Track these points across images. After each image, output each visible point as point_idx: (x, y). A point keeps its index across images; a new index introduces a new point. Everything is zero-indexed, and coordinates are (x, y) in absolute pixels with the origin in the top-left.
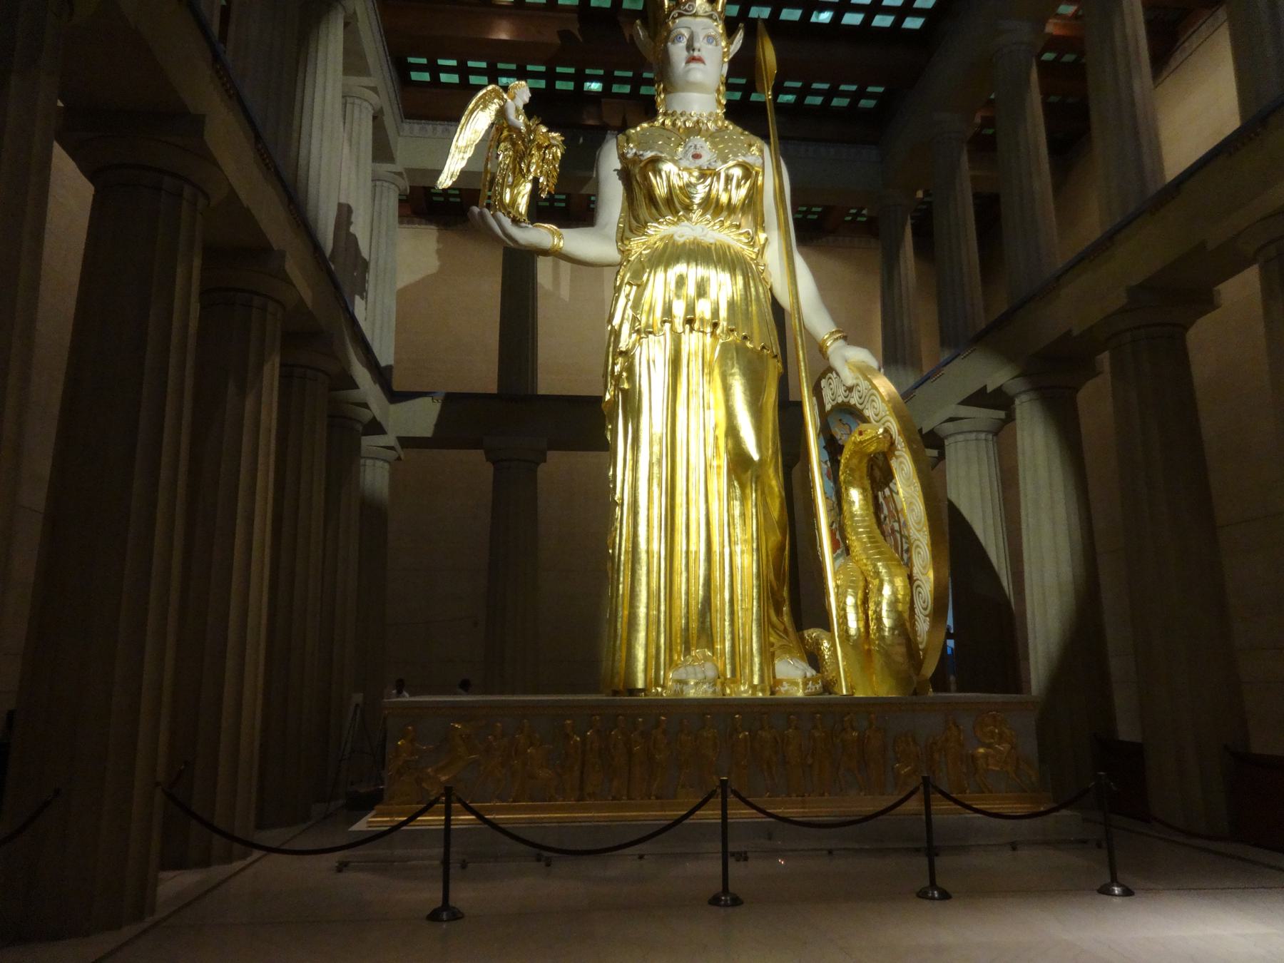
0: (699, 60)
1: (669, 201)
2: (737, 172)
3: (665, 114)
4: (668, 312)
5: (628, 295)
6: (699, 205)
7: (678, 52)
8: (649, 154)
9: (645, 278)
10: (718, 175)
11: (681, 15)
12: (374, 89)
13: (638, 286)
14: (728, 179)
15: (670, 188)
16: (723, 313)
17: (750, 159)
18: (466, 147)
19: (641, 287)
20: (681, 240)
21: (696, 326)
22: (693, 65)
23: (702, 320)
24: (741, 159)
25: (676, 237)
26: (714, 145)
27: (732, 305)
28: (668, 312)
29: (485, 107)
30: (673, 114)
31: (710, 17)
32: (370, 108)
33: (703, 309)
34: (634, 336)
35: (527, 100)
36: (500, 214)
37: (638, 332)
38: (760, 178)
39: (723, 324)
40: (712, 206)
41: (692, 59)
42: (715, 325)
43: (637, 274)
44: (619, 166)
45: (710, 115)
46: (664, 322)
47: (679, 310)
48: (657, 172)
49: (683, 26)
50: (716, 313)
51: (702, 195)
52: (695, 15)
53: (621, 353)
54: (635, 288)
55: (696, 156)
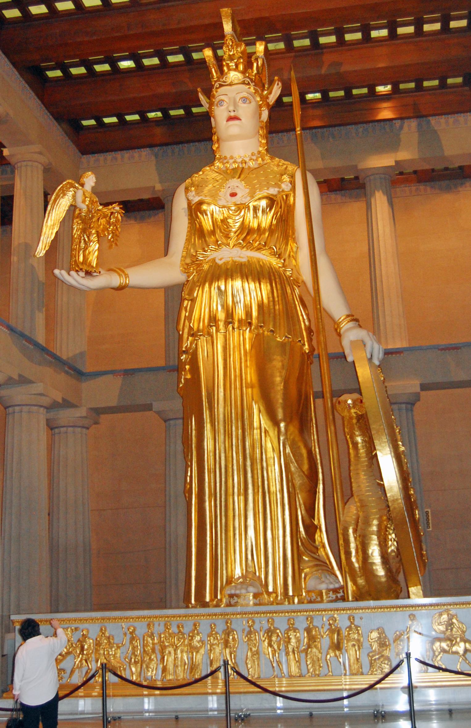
0: (236, 118)
1: (213, 233)
2: (263, 203)
3: (220, 159)
4: (213, 319)
5: (186, 308)
6: (235, 232)
7: (220, 115)
8: (196, 199)
9: (195, 295)
10: (248, 208)
11: (221, 86)
12: (40, 153)
13: (192, 300)
14: (255, 209)
15: (214, 222)
16: (255, 314)
17: (273, 191)
18: (54, 225)
19: (193, 301)
20: (220, 262)
21: (236, 325)
22: (231, 123)
23: (240, 321)
24: (265, 193)
25: (217, 261)
26: (249, 183)
27: (261, 306)
28: (213, 319)
29: (65, 195)
30: (225, 158)
31: (243, 83)
32: (40, 166)
33: (240, 312)
34: (190, 338)
35: (93, 184)
36: (73, 273)
37: (192, 335)
38: (292, 199)
39: (254, 321)
40: (246, 232)
41: (230, 119)
42: (250, 324)
43: (191, 292)
44: (185, 205)
45: (253, 154)
46: (211, 326)
47: (221, 315)
48: (204, 212)
49: (220, 93)
50: (249, 314)
51: (238, 225)
52: (230, 85)
53: (184, 351)
54: (190, 302)
55: (233, 195)
